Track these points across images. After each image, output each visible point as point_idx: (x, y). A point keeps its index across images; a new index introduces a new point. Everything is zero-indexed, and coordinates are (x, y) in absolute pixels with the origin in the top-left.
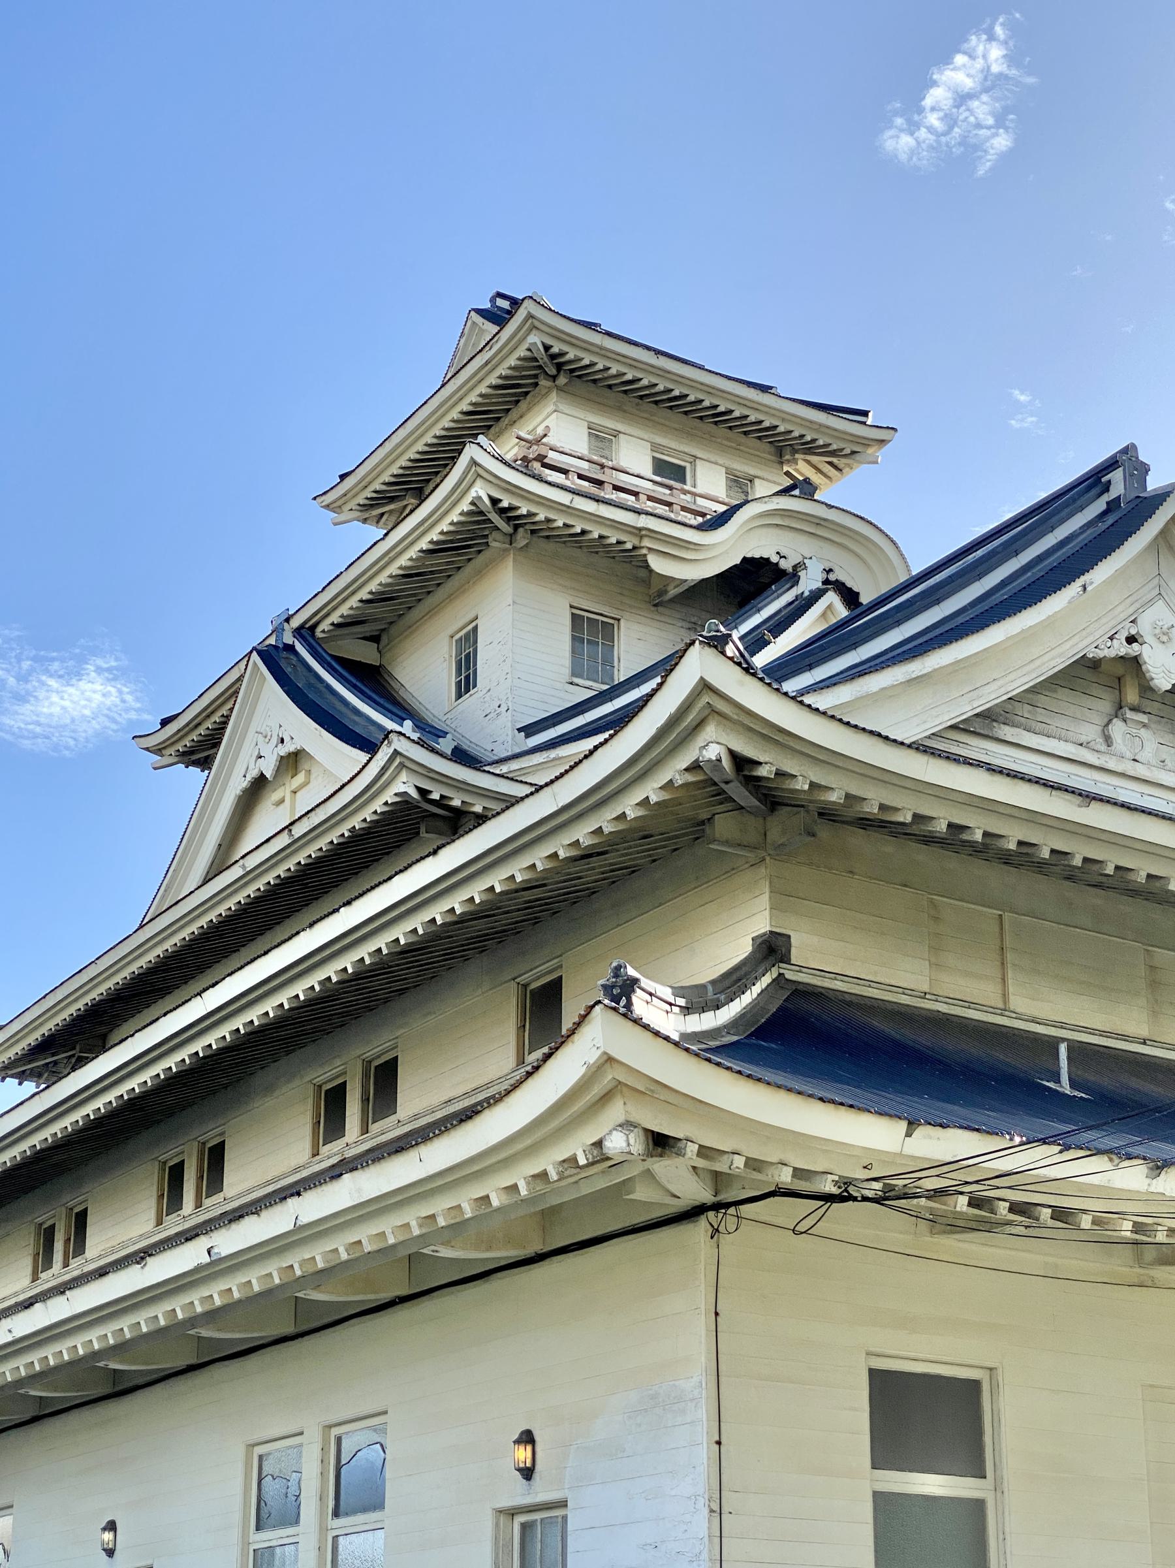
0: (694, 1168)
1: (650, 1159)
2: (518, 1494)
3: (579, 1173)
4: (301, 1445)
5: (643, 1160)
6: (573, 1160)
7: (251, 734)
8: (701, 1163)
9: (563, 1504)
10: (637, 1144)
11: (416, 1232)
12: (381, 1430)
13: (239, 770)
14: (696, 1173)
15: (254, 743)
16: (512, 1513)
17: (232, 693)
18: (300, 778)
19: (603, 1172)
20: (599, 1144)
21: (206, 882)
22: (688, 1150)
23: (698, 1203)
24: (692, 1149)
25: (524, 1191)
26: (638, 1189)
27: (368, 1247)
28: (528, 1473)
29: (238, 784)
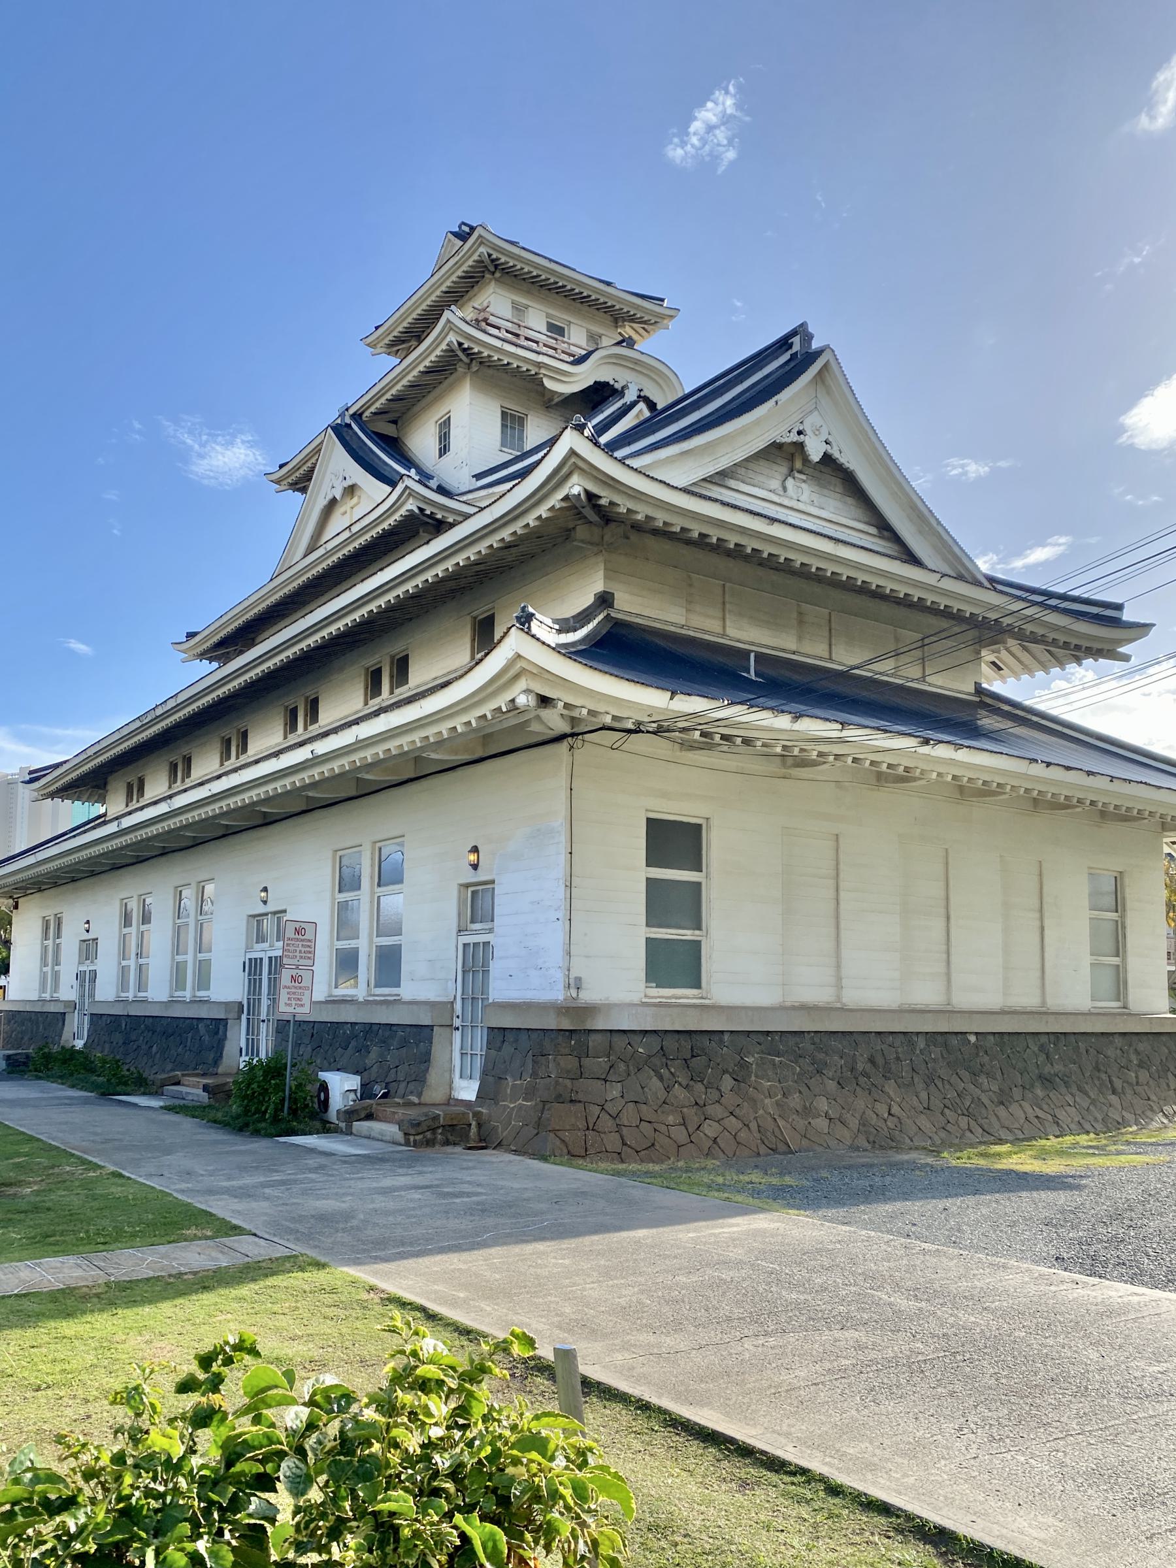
2: (470, 877)
4: (360, 852)
6: (500, 708)
7: (328, 476)
8: (565, 712)
9: (493, 882)
10: (532, 701)
11: (419, 745)
12: (402, 844)
13: (322, 495)
16: (467, 886)
17: (317, 450)
18: (355, 500)
20: (513, 701)
21: (305, 556)
24: (560, 704)
25: (474, 725)
27: (394, 752)
28: (475, 867)
29: (322, 502)
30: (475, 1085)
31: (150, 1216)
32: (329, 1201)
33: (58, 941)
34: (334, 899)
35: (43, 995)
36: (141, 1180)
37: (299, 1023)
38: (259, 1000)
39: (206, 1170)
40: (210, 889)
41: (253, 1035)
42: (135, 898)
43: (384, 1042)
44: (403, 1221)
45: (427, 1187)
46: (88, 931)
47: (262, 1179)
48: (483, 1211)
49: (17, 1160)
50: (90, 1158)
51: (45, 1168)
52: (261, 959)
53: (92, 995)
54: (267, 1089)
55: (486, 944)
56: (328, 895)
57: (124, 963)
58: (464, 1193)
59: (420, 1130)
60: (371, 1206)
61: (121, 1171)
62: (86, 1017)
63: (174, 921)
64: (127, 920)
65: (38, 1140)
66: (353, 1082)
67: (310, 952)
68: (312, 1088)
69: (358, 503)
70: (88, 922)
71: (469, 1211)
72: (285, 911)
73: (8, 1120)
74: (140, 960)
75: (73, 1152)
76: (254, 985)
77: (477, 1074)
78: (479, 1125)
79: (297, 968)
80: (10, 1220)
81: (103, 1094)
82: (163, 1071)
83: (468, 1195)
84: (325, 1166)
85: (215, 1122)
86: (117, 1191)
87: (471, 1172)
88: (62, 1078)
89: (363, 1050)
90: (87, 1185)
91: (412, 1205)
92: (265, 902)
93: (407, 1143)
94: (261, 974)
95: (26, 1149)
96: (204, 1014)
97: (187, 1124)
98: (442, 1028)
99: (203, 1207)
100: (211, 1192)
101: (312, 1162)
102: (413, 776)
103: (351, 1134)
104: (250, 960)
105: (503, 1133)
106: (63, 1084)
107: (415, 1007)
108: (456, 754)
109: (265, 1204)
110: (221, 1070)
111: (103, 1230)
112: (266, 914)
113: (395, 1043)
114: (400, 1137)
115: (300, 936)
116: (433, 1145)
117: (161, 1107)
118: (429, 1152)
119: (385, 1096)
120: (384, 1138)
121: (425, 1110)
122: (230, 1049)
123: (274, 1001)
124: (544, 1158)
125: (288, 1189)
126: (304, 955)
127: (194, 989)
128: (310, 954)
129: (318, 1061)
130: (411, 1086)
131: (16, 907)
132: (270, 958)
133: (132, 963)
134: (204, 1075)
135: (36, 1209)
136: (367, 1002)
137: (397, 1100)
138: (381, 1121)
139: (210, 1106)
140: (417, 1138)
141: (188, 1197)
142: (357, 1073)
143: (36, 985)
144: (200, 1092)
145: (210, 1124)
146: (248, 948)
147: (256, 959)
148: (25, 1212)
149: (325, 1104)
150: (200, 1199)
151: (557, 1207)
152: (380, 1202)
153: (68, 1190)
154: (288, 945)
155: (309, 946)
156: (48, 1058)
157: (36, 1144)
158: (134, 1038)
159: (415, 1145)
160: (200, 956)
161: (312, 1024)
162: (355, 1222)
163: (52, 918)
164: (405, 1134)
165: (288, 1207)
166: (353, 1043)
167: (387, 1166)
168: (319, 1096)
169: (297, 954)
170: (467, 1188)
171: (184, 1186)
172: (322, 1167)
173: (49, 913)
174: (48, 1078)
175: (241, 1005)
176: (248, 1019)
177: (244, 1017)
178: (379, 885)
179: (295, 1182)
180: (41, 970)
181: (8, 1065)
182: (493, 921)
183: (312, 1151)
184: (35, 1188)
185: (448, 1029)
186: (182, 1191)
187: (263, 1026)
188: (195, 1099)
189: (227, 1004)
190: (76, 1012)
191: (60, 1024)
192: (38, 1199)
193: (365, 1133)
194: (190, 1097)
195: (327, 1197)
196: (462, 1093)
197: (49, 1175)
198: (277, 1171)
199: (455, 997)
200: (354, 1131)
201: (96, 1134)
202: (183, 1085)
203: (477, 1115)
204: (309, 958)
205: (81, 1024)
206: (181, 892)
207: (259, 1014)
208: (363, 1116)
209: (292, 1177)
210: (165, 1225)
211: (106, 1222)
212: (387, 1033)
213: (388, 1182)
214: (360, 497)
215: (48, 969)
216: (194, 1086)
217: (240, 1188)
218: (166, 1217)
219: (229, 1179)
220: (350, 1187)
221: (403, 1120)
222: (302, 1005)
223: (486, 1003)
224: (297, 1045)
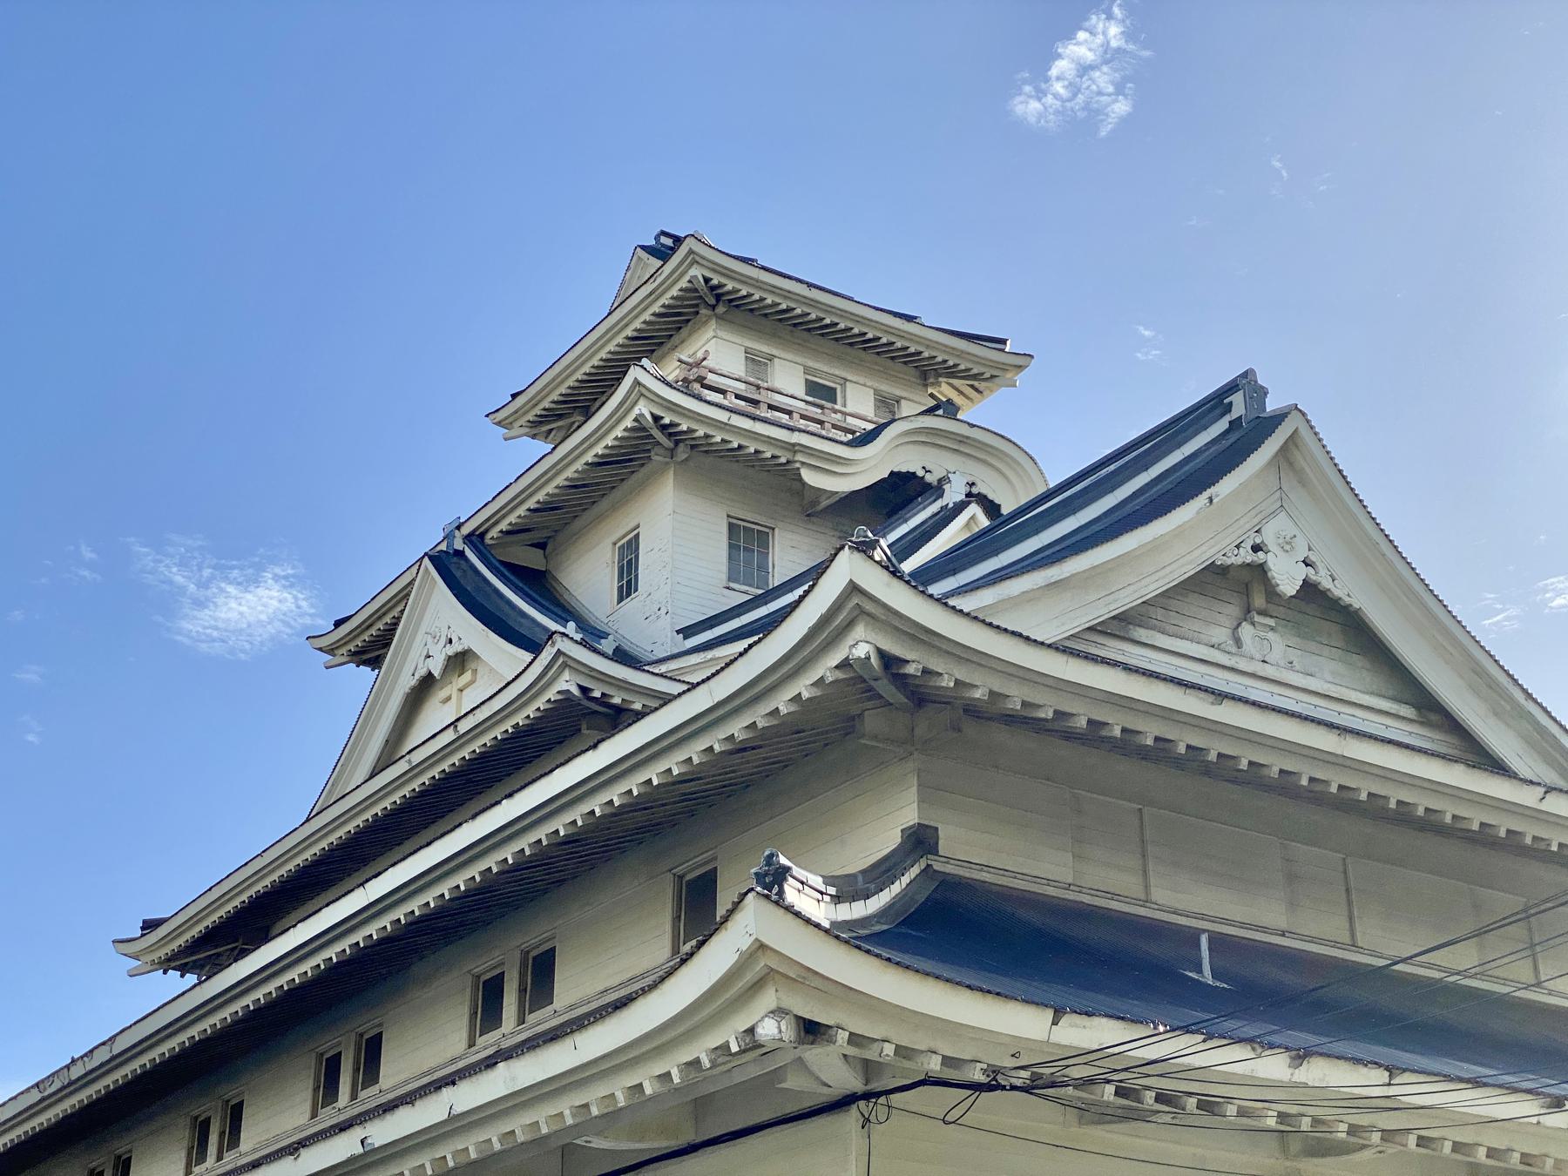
0: (845, 1056)
1: (801, 1047)
3: (730, 1061)
5: (795, 1048)
6: (725, 1047)
7: (420, 636)
8: (852, 1051)
10: (788, 1031)
11: (569, 1121)
14: (847, 1061)
17: (403, 596)
18: (467, 676)
19: (755, 1060)
20: (751, 1031)
21: (372, 776)
22: (839, 1037)
23: (849, 1093)
24: (842, 1036)
25: (676, 1080)
26: (789, 1076)
27: (521, 1138)
29: (407, 682)
69: (472, 682)
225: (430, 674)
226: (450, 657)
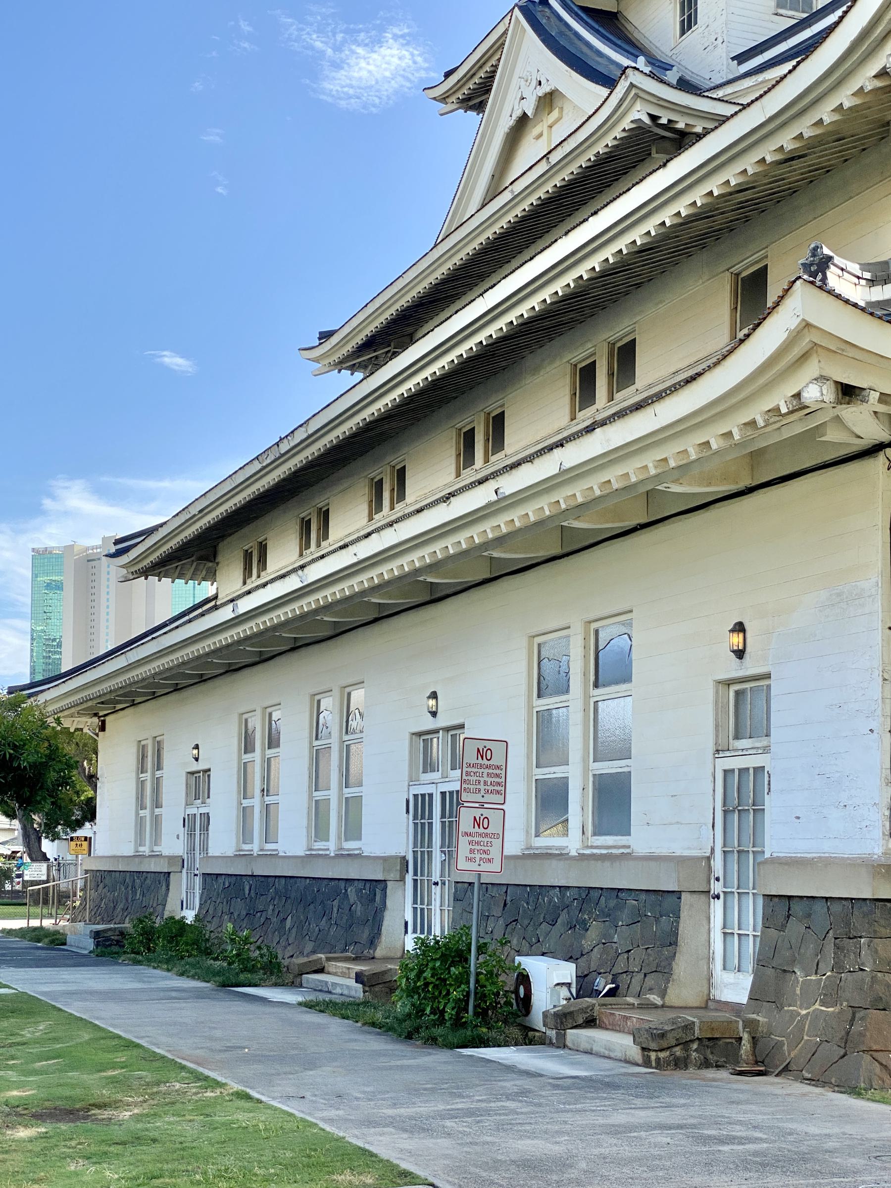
0: (875, 413)
1: (839, 407)
2: (733, 669)
3: (781, 420)
4: (569, 636)
5: (833, 407)
6: (777, 409)
7: (515, 81)
8: (881, 408)
9: (768, 676)
10: (829, 394)
11: (653, 472)
12: (629, 624)
14: (877, 417)
15: (518, 87)
16: (728, 683)
17: (499, 45)
19: (800, 419)
20: (798, 396)
21: (483, 206)
22: (871, 397)
23: (877, 442)
24: (874, 396)
25: (737, 437)
26: (828, 432)
27: (615, 485)
28: (740, 654)
29: (506, 123)
30: (746, 981)
31: (289, 1154)
32: (536, 1141)
33: (158, 774)
34: (530, 707)
35: (141, 849)
36: (275, 1103)
37: (486, 887)
38: (430, 853)
39: (364, 1092)
40: (358, 696)
41: (422, 903)
42: (259, 712)
43: (609, 916)
44: (645, 1175)
45: (680, 1127)
46: (197, 759)
47: (441, 1107)
48: (764, 1165)
49: (110, 1073)
50: (207, 1072)
51: (148, 1084)
52: (431, 795)
53: (205, 848)
54: (445, 980)
55: (759, 770)
56: (522, 701)
57: (246, 803)
58: (734, 1138)
59: (665, 1044)
60: (596, 1151)
61: (248, 1090)
62: (197, 879)
63: (311, 743)
64: (248, 746)
65: (138, 1046)
66: (567, 971)
67: (499, 784)
68: (508, 980)
70: (197, 747)
71: (744, 1164)
72: (462, 726)
73: (98, 1018)
74: (266, 798)
75: (184, 1063)
76: (422, 832)
77: (749, 965)
78: (754, 1040)
79: (482, 807)
80: (106, 1153)
81: (224, 985)
82: (302, 953)
83: (741, 1141)
84: (530, 1091)
85: (373, 1024)
86: (242, 1118)
87: (743, 1107)
88: (168, 963)
89: (579, 926)
90: (204, 1109)
91: (655, 1152)
92: (434, 714)
93: (647, 1063)
94: (431, 817)
95: (121, 1057)
96: (353, 873)
97: (335, 1025)
98: (695, 896)
99: (360, 1144)
100: (370, 1122)
101: (511, 1084)
102: (644, 520)
103: (565, 1046)
104: (416, 796)
105: (790, 1053)
106: (168, 970)
107: (653, 864)
108: (709, 484)
109: (444, 1142)
110: (379, 952)
111: (226, 1170)
112: (436, 731)
113: (624, 917)
114: (635, 1053)
115: (485, 762)
116: (686, 1067)
117: (300, 1004)
118: (678, 1076)
119: (612, 993)
120: (612, 1055)
121: (671, 1015)
122: (391, 924)
123: (450, 855)
124: (855, 1091)
125: (478, 1122)
126: (490, 788)
127: (339, 838)
128: (500, 787)
129: (515, 942)
130: (650, 981)
131: (103, 728)
132: (443, 794)
133: (256, 802)
134: (356, 959)
135: (137, 1140)
136: (582, 857)
137: (630, 1000)
138: (607, 1029)
139: (365, 1003)
140: (662, 1055)
141: (339, 1128)
142: (569, 959)
143: (131, 834)
144: (352, 982)
145: (366, 1028)
146: (413, 780)
147: (423, 796)
148: (123, 1143)
149: (526, 1003)
150: (356, 1132)
151: (878, 1164)
152: (610, 1146)
153: (179, 1115)
154: (468, 774)
155: (497, 776)
156: (148, 936)
157: (135, 1052)
158: (261, 908)
159: (659, 1065)
160: (348, 792)
161: (504, 889)
162: (573, 1174)
163: (149, 743)
164: (643, 1049)
165: (478, 1148)
166: (563, 917)
167: (618, 1094)
168: (516, 992)
169: (482, 787)
170: (739, 1131)
171: (333, 1113)
172: (524, 1093)
173: (146, 736)
174: (149, 962)
175: (404, 861)
176: (415, 881)
177: (409, 878)
178: (596, 685)
179: (488, 1112)
180: (137, 814)
181: (97, 945)
182: (768, 735)
183: (510, 1069)
184: (136, 1111)
185: (703, 897)
186: (330, 1121)
187: (436, 891)
188: (346, 992)
189: (385, 859)
190: (184, 871)
191: (164, 887)
192: (139, 1126)
193: (584, 1046)
194: (338, 990)
195: (532, 1135)
196: (725, 991)
197: (153, 1094)
198: (460, 1096)
199: (713, 850)
200: (569, 1043)
201: (211, 1039)
202: (329, 973)
203: (750, 1025)
204: (498, 792)
205: (190, 889)
206: (319, 701)
207: (430, 874)
208: (580, 1021)
209: (484, 1105)
210: (309, 1166)
211: (229, 1161)
212: (612, 903)
213: (620, 1118)
214: (561, 109)
215: (145, 813)
216: (344, 975)
217: (411, 1118)
218: (309, 1157)
219: (394, 1106)
220: (565, 1122)
221: (639, 1030)
222: (490, 860)
223: (760, 859)
224: (484, 918)
225: (525, 114)
226: (540, 97)
